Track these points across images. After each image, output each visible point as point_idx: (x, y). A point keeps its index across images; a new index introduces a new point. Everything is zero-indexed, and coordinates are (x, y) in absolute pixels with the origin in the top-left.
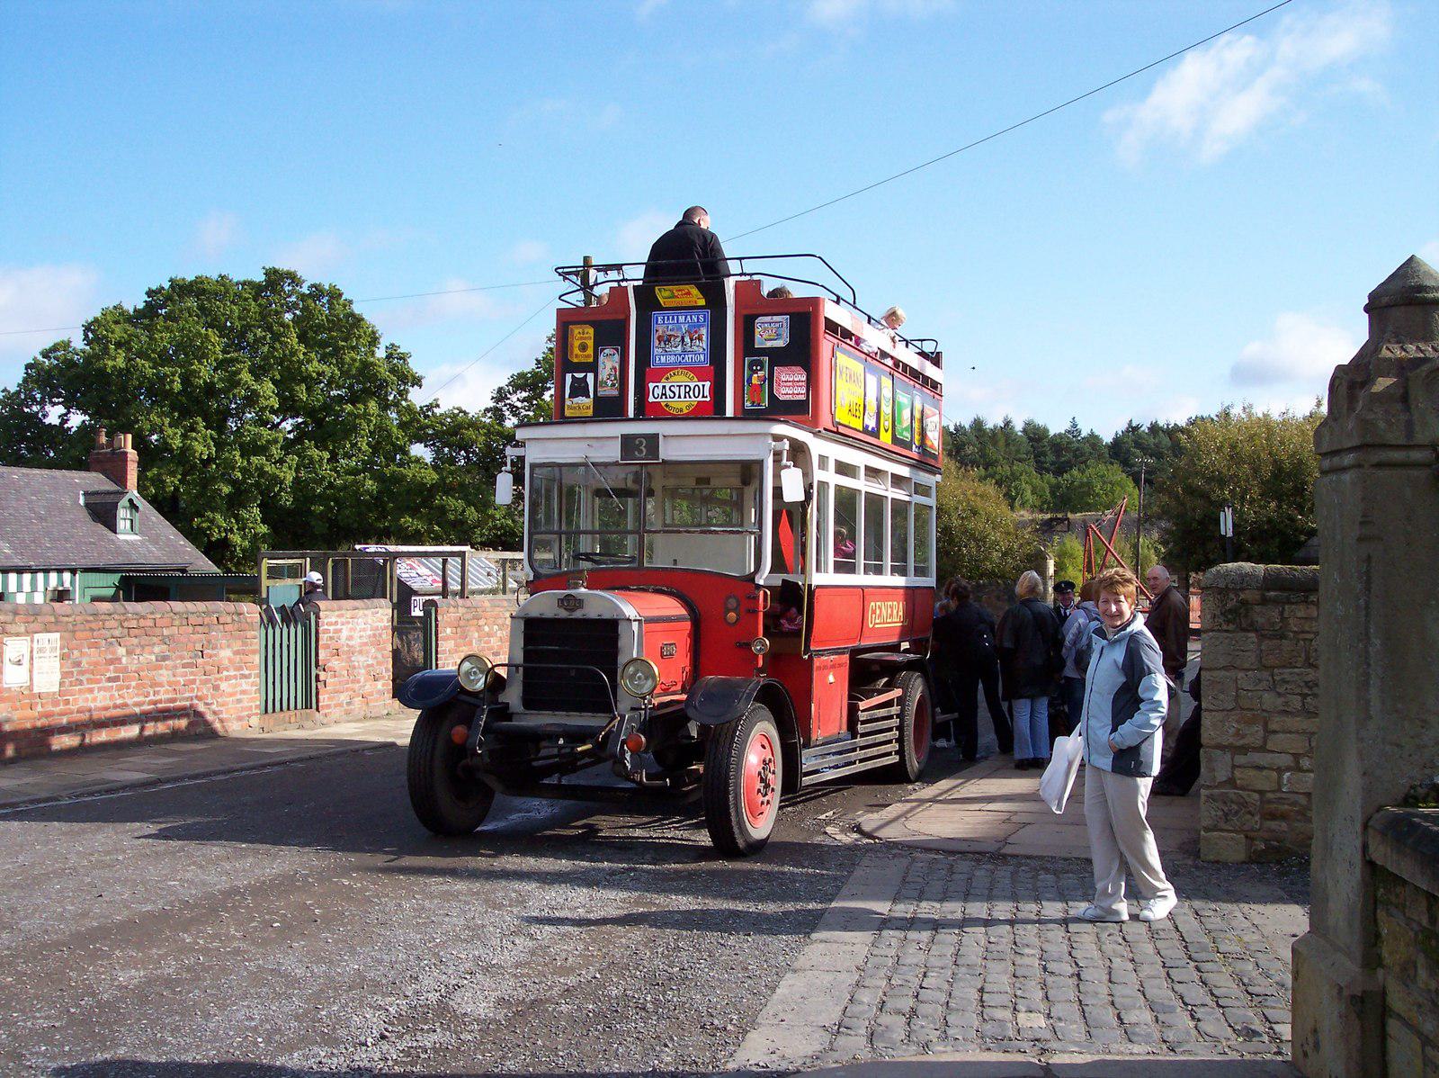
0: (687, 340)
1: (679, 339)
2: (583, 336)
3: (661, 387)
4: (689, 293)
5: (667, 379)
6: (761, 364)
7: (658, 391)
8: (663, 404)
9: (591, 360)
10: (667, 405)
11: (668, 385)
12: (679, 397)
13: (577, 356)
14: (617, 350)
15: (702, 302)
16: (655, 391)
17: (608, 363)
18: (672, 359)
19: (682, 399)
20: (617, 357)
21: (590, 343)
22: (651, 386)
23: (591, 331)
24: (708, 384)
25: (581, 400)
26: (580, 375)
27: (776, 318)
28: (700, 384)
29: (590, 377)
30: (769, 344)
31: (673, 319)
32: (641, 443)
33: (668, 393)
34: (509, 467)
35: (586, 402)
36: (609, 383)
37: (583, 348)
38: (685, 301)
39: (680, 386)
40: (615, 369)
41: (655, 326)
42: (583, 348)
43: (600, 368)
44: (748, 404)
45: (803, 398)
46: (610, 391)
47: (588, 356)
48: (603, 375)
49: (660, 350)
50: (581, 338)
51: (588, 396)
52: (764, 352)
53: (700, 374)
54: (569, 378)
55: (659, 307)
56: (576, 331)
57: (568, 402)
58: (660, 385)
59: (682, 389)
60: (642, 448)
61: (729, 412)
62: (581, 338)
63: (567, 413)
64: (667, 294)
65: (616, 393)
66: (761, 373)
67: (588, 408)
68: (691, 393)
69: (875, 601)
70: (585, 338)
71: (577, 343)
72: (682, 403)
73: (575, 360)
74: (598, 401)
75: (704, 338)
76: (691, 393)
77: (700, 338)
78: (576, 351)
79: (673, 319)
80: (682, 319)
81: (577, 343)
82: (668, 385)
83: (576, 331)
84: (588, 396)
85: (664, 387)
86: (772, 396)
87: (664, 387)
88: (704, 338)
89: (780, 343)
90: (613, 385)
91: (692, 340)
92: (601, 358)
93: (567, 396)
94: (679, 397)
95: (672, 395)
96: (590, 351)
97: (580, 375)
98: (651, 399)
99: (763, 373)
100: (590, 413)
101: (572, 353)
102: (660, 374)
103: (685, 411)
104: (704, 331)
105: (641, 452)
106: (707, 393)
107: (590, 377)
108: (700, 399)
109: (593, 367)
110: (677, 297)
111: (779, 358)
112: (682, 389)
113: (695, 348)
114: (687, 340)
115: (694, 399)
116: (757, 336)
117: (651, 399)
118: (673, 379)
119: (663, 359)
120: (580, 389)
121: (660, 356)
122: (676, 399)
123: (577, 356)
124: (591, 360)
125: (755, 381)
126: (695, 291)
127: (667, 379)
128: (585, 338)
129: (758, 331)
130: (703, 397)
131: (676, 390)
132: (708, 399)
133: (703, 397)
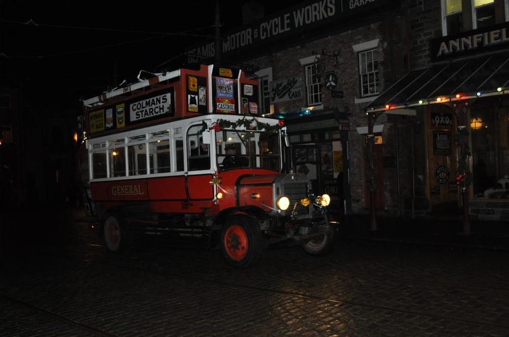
0: (227, 89)
4: (228, 72)
6: (246, 100)
7: (220, 106)
15: (231, 76)
16: (219, 105)
17: (202, 93)
18: (223, 95)
20: (205, 91)
21: (196, 84)
22: (218, 104)
23: (196, 80)
24: (234, 105)
25: (193, 105)
26: (193, 96)
27: (249, 86)
29: (196, 97)
30: (248, 94)
37: (194, 86)
38: (227, 75)
41: (217, 83)
42: (194, 86)
43: (200, 94)
47: (195, 89)
48: (201, 97)
51: (196, 104)
53: (231, 102)
54: (189, 96)
55: (219, 76)
56: (191, 79)
57: (189, 106)
63: (190, 110)
65: (205, 104)
71: (192, 83)
73: (191, 90)
74: (199, 106)
75: (232, 89)
77: (230, 89)
78: (192, 87)
81: (192, 83)
83: (191, 79)
88: (232, 89)
89: (250, 94)
92: (200, 91)
93: (189, 103)
96: (196, 87)
97: (193, 96)
98: (218, 109)
100: (197, 111)
104: (231, 87)
107: (196, 97)
109: (197, 93)
114: (227, 89)
116: (245, 91)
121: (220, 94)
123: (192, 88)
124: (196, 91)
131: (225, 106)
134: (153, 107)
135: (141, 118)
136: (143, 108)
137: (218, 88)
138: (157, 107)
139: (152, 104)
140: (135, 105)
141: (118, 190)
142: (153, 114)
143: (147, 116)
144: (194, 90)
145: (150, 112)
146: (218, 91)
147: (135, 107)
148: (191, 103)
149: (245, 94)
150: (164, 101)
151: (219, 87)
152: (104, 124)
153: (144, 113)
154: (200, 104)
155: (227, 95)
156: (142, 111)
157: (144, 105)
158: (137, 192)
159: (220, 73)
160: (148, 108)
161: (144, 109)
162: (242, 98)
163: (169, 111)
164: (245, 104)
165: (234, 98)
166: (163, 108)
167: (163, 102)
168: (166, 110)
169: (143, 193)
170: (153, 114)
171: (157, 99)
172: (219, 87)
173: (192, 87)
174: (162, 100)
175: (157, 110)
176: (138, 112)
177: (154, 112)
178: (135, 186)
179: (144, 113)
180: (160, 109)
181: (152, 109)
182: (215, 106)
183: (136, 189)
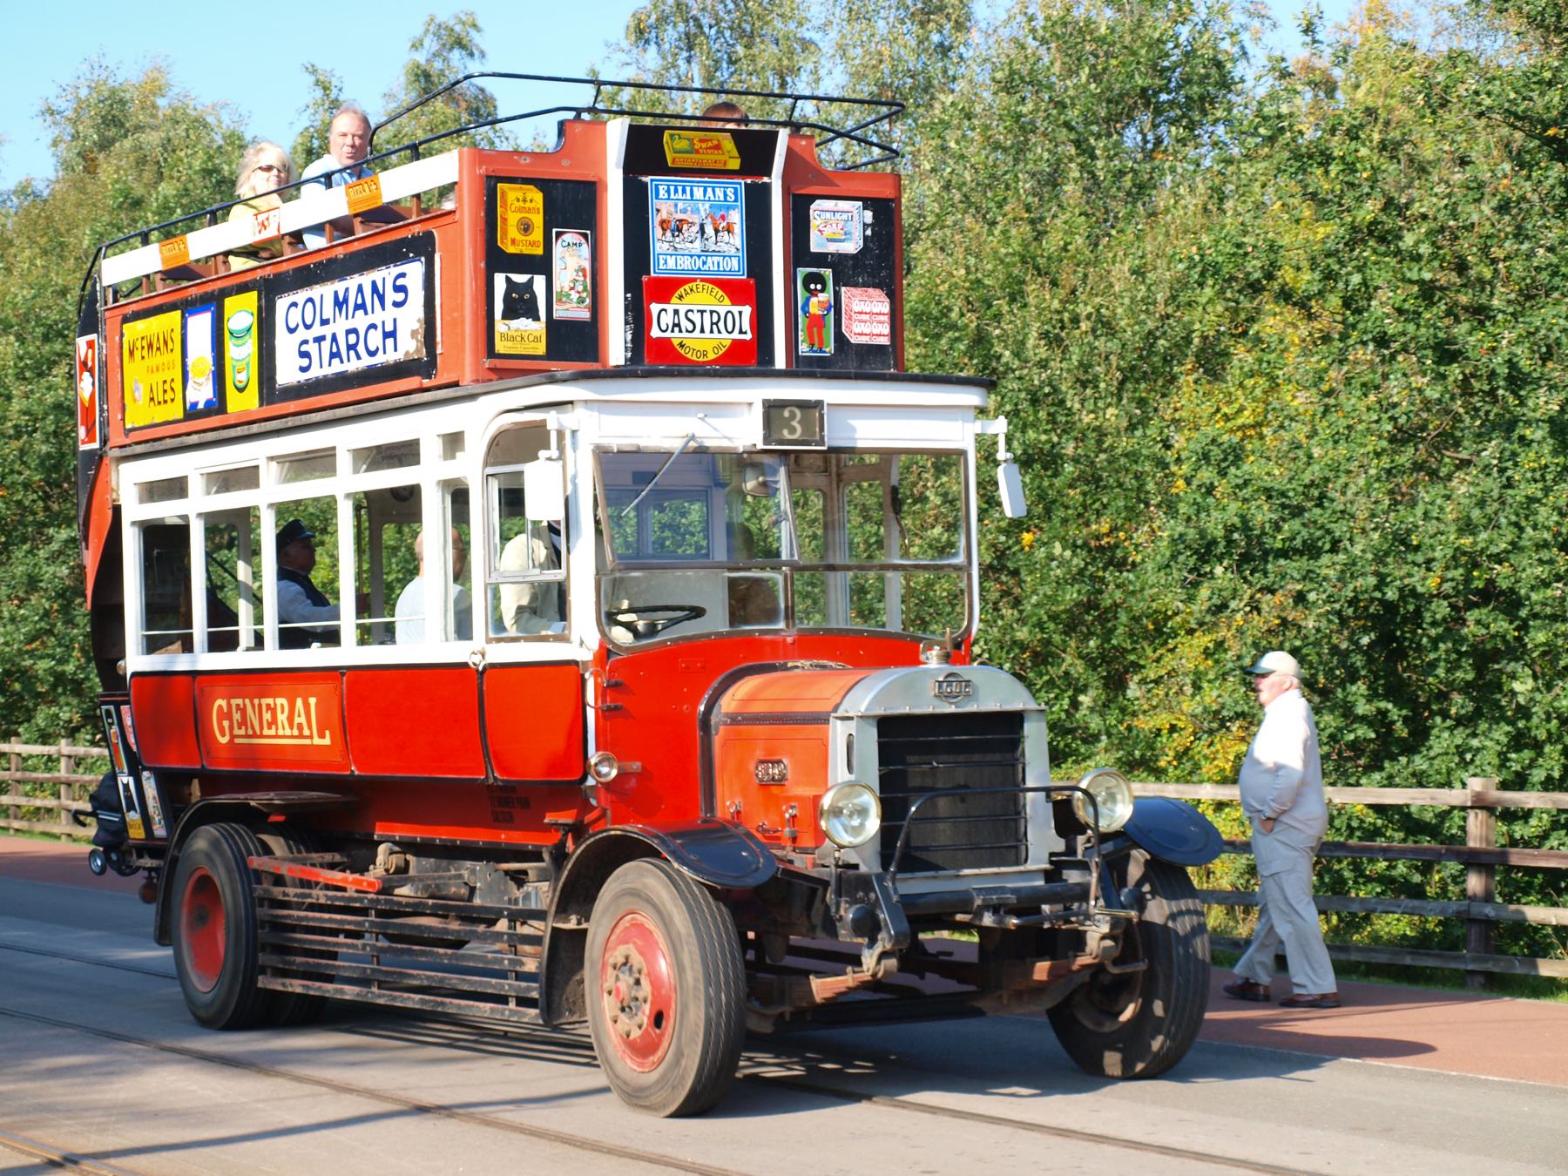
0: (709, 230)
1: (697, 228)
2: (522, 208)
3: (671, 313)
4: (718, 147)
5: (681, 297)
6: (819, 279)
7: (667, 319)
8: (676, 342)
9: (540, 251)
10: (681, 345)
11: (682, 310)
12: (702, 331)
13: (513, 241)
14: (585, 236)
15: (735, 164)
17: (570, 257)
18: (686, 263)
19: (707, 334)
20: (585, 250)
21: (538, 220)
22: (655, 308)
23: (537, 197)
24: (747, 310)
25: (523, 324)
26: (520, 278)
28: (735, 309)
29: (539, 283)
30: (832, 248)
31: (684, 191)
32: (793, 416)
33: (685, 324)
34: (554, 452)
35: (523, 335)
36: (575, 296)
37: (526, 228)
38: (709, 160)
39: (702, 312)
40: (584, 270)
41: (653, 203)
42: (526, 228)
44: (804, 348)
45: (885, 341)
46: (573, 310)
47: (532, 244)
49: (666, 246)
50: (521, 210)
51: (537, 318)
52: (821, 259)
53: (734, 291)
54: (500, 280)
55: (663, 169)
57: (500, 326)
58: (670, 308)
59: (707, 316)
60: (794, 423)
61: (780, 362)
62: (521, 210)
63: (501, 347)
64: (684, 144)
65: (584, 315)
66: (822, 297)
67: (537, 339)
68: (721, 324)
69: (229, 697)
70: (529, 210)
72: (705, 344)
73: (511, 250)
74: (554, 326)
75: (737, 229)
76: (721, 324)
77: (729, 230)
78: (513, 232)
79: (684, 191)
80: (698, 193)
81: (513, 219)
82: (682, 310)
84: (537, 318)
85: (676, 312)
86: (840, 338)
87: (676, 312)
88: (737, 229)
89: (852, 247)
90: (581, 300)
91: (717, 231)
92: (558, 250)
94: (702, 331)
95: (690, 327)
96: (538, 234)
98: (655, 333)
99: (826, 297)
100: (541, 349)
101: (505, 232)
102: (667, 289)
103: (711, 356)
105: (792, 430)
106: (746, 326)
108: (736, 335)
109: (543, 264)
110: (697, 152)
111: (848, 270)
112: (707, 316)
113: (723, 247)
114: (709, 230)
115: (725, 335)
117: (655, 333)
118: (687, 299)
119: (671, 262)
120: (520, 305)
121: (666, 257)
122: (697, 333)
124: (540, 251)
125: (814, 309)
126: (729, 144)
127: (681, 297)
128: (529, 210)
129: (816, 221)
130: (741, 332)
131: (696, 317)
132: (748, 337)
133: (741, 332)
134: (360, 321)
135: (316, 372)
136: (325, 322)
137: (656, 232)
138: (373, 326)
139: (357, 307)
140: (295, 304)
141: (237, 716)
142: (359, 357)
143: (337, 367)
144: (527, 251)
145: (350, 347)
146: (659, 244)
147: (295, 317)
148: (505, 316)
149: (814, 248)
150: (400, 297)
151: (663, 222)
152: (178, 386)
153: (326, 345)
154: (560, 312)
155: (712, 263)
156: (319, 340)
157: (328, 312)
158: (306, 732)
159: (669, 157)
160: (340, 326)
161: (327, 331)
162: (802, 272)
163: (417, 350)
164: (814, 300)
165: (751, 272)
166: (392, 334)
167: (397, 304)
168: (408, 346)
169: (327, 741)
170: (359, 357)
171: (374, 284)
172: (664, 224)
173: (513, 232)
174: (391, 296)
175: (375, 339)
176: (305, 342)
177: (361, 348)
178: (299, 702)
179: (326, 345)
180: (386, 335)
181: (355, 331)
182: (637, 317)
183: (302, 720)
